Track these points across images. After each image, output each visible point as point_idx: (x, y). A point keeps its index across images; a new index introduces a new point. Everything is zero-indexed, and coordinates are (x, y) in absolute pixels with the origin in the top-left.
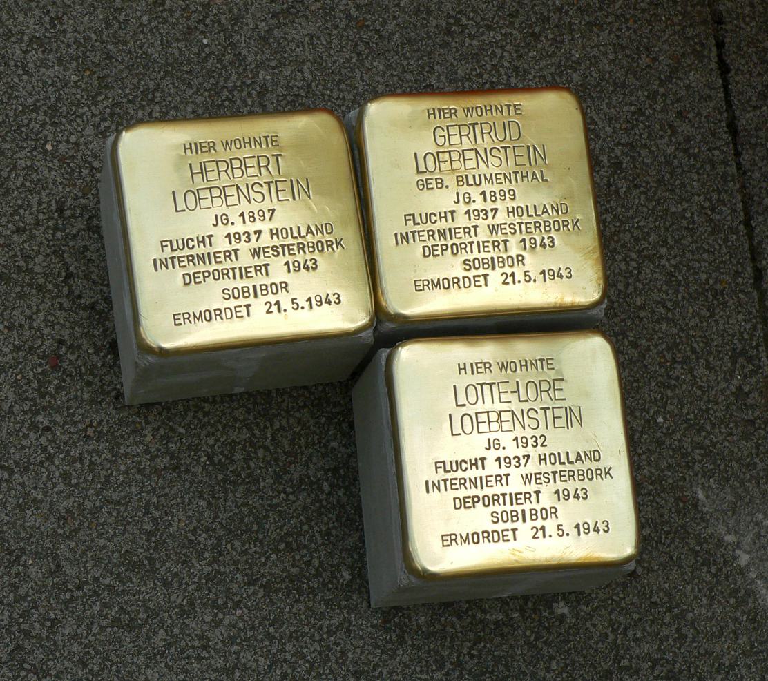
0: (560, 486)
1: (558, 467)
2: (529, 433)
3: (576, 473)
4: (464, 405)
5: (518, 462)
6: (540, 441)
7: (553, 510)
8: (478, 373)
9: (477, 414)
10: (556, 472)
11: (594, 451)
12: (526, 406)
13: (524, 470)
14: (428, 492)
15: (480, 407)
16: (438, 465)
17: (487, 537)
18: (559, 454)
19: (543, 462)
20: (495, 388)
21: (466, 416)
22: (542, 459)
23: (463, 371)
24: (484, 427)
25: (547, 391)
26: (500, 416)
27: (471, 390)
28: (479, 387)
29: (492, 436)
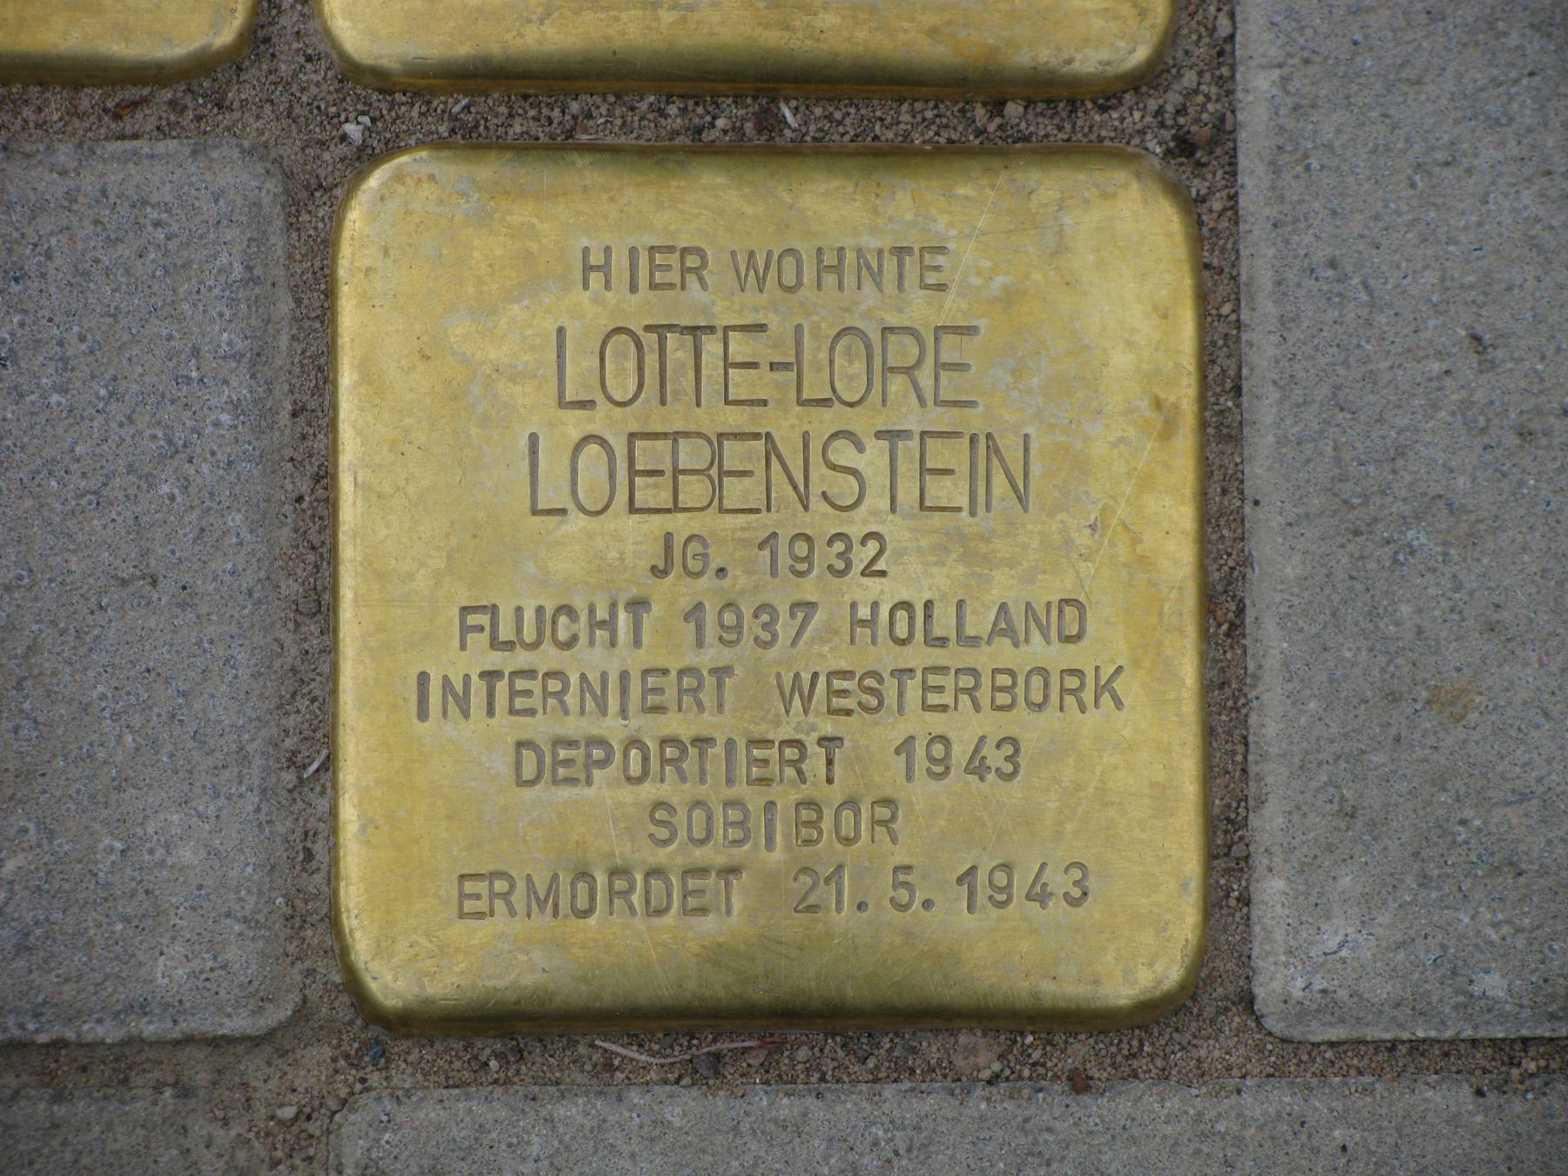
1: (917, 656)
2: (821, 521)
3: (986, 682)
8: (653, 286)
12: (824, 422)
14: (423, 715)
16: (473, 619)
21: (593, 448)
25: (908, 371)
26: (717, 456)
29: (681, 525)
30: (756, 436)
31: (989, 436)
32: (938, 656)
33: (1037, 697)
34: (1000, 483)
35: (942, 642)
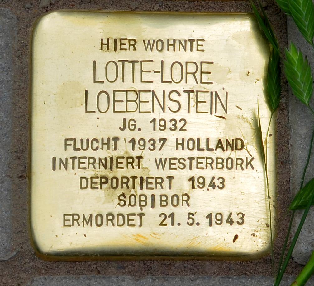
0: (196, 173)
1: (195, 153)
2: (168, 116)
3: (215, 162)
4: (102, 82)
5: (153, 145)
6: (179, 125)
7: (185, 198)
9: (115, 91)
10: (193, 158)
11: (237, 139)
12: (168, 88)
13: (158, 154)
15: (118, 85)
16: (68, 142)
17: (112, 220)
18: (199, 140)
19: (180, 147)
20: (137, 66)
21: (104, 94)
22: (180, 144)
23: (105, 47)
24: (120, 107)
25: (193, 74)
27: (112, 67)
28: (120, 65)
29: (128, 116)
30: (150, 91)
31: (216, 93)
32: (201, 154)
33: (229, 166)
34: (219, 106)
35: (203, 150)
